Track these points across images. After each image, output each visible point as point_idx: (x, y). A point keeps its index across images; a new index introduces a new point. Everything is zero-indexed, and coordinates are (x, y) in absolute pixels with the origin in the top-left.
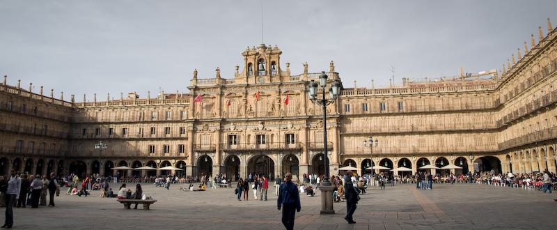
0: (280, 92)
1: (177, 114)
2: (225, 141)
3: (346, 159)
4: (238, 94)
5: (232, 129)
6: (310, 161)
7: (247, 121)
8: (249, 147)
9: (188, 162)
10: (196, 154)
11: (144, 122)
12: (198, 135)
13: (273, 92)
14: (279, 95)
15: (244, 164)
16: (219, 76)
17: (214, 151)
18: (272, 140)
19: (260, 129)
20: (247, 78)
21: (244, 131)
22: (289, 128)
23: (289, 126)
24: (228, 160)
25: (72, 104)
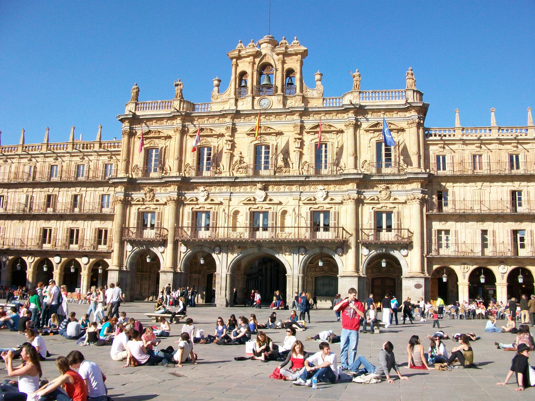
0: (302, 128)
1: (96, 169)
2: (186, 221)
3: (435, 267)
4: (218, 130)
5: (202, 200)
6: (362, 268)
8: (234, 236)
9: (112, 262)
10: (128, 248)
11: (35, 185)
14: (301, 133)
18: (283, 223)
19: (259, 199)
20: (236, 100)
21: (226, 203)
22: (320, 200)
24: (191, 262)
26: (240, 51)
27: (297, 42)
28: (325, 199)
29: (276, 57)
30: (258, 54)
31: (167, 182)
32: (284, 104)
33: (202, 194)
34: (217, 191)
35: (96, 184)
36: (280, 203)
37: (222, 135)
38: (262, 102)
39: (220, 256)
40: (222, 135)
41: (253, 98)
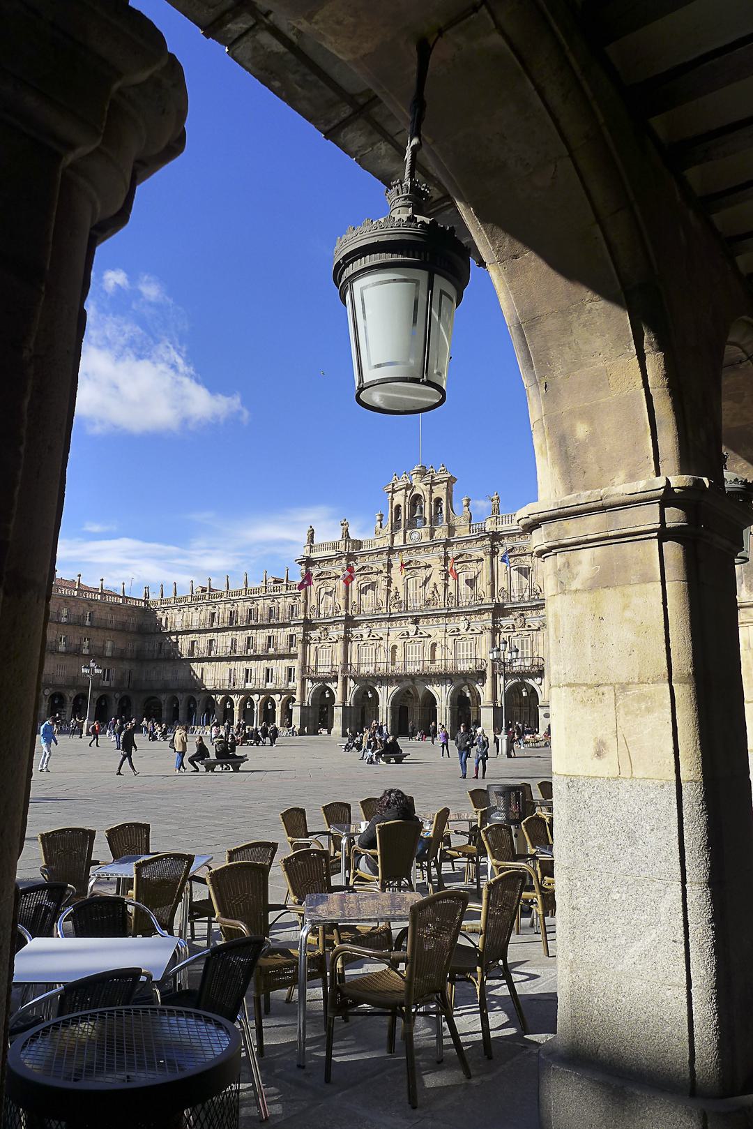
7: (390, 620)
10: (309, 684)
11: (237, 629)
12: (313, 647)
13: (433, 559)
14: (446, 565)
15: (385, 703)
16: (346, 535)
17: (336, 679)
20: (393, 536)
21: (385, 637)
23: (463, 626)
25: (146, 602)
26: (393, 485)
27: (443, 468)
28: (467, 630)
29: (424, 487)
30: (409, 487)
31: (335, 621)
32: (432, 536)
33: (365, 631)
34: (378, 627)
35: (284, 625)
36: (430, 636)
37: (381, 572)
38: (415, 536)
39: (381, 689)
40: (381, 572)
41: (405, 533)
